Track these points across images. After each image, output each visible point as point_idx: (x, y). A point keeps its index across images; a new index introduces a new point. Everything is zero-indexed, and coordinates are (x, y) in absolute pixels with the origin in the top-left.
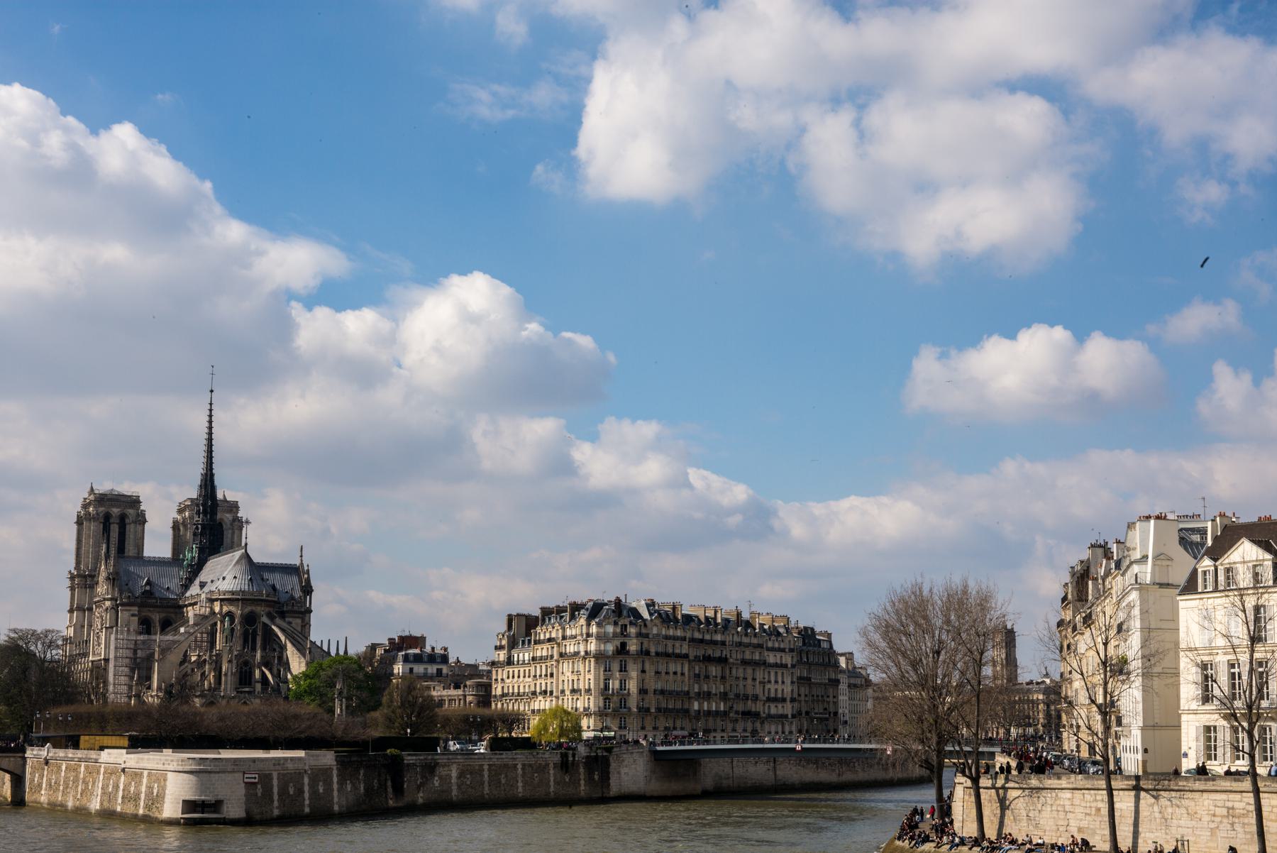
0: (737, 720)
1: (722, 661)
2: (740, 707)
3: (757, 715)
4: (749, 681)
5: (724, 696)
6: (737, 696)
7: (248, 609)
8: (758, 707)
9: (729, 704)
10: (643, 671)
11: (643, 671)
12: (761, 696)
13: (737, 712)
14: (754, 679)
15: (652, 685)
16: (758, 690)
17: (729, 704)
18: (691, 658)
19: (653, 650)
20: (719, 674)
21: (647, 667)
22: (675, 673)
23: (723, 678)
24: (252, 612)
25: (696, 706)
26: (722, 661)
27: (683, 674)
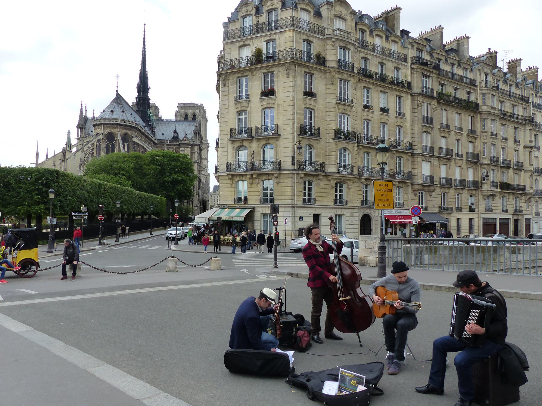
0: (493, 196)
1: (471, 108)
2: (496, 176)
3: (522, 190)
4: (511, 143)
5: (474, 160)
6: (494, 160)
7: (107, 131)
8: (524, 179)
9: (481, 172)
10: (309, 94)
11: (309, 94)
12: (527, 166)
13: (493, 184)
14: (517, 142)
15: (328, 120)
16: (524, 157)
17: (481, 172)
18: (416, 89)
19: (332, 56)
20: (467, 126)
21: (320, 85)
22: (384, 110)
23: (472, 132)
24: (111, 132)
25: (425, 169)
26: (471, 108)
27: (400, 114)
